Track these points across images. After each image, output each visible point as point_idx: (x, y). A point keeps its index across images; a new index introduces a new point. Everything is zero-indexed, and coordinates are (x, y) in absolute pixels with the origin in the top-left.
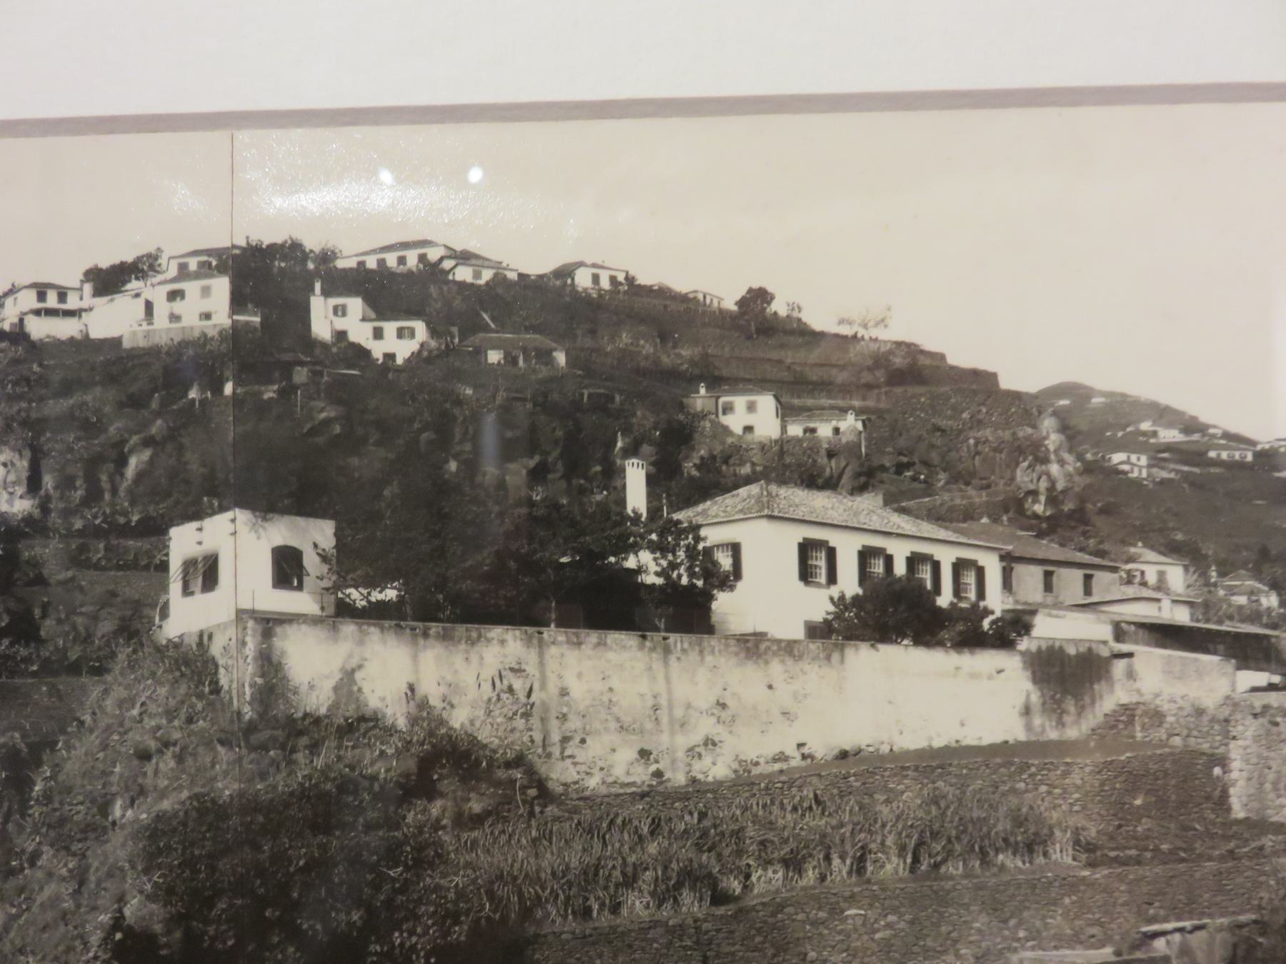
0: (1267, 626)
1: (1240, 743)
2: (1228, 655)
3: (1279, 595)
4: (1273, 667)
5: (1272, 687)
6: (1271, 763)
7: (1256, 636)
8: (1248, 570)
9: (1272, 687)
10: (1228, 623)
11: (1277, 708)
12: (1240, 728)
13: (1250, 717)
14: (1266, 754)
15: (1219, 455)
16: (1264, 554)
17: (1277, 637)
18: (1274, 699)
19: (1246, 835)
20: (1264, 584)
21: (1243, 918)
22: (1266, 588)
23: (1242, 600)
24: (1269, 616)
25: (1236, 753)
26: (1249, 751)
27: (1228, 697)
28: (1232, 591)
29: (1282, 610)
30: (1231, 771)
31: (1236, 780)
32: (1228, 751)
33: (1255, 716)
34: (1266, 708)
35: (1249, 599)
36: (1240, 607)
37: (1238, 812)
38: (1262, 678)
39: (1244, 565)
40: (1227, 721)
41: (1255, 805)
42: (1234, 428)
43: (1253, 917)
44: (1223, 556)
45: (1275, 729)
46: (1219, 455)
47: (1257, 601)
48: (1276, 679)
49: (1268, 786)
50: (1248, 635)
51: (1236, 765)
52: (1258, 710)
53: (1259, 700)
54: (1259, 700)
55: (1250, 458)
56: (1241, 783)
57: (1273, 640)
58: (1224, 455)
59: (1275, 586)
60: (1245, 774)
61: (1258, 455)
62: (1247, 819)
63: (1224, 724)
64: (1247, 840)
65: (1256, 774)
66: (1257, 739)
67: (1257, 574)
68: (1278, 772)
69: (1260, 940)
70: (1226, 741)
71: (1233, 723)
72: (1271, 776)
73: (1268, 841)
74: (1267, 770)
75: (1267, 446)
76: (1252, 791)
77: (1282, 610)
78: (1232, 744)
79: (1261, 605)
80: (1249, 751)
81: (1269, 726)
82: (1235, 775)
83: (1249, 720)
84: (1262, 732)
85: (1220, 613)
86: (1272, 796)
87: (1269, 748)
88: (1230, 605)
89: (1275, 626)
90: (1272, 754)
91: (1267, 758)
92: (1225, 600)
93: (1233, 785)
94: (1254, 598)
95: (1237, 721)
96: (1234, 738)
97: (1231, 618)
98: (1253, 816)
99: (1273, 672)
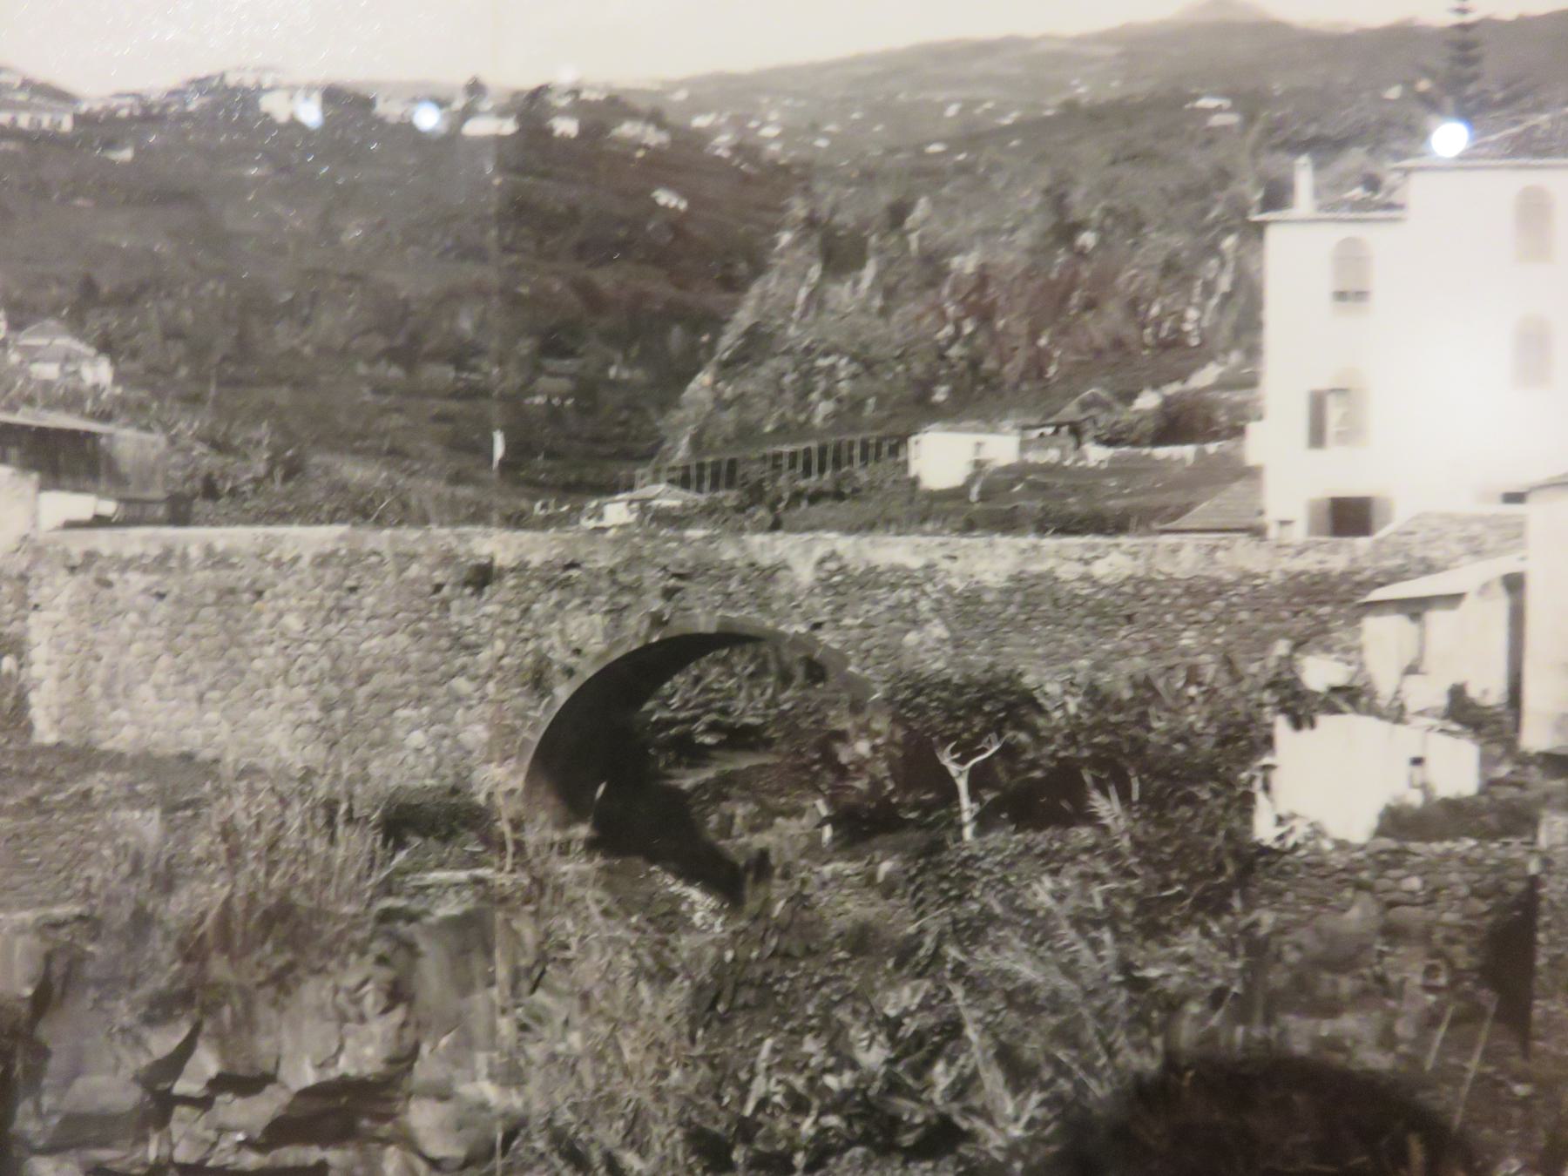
0: (93, 416)
1: (47, 615)
2: (27, 465)
3: (114, 362)
4: (103, 486)
5: (99, 521)
6: (100, 650)
7: (74, 435)
8: (61, 319)
9: (99, 521)
10: (24, 409)
11: (110, 557)
12: (46, 591)
13: (63, 573)
14: (90, 634)
15: (14, 120)
16: (89, 288)
17: (110, 436)
18: (103, 541)
19: (61, 772)
20: (90, 344)
21: (60, 911)
22: (91, 351)
23: (48, 371)
24: (97, 398)
25: (39, 631)
26: (61, 629)
27: (25, 538)
28: (31, 354)
29: (119, 390)
30: (31, 664)
31: (41, 681)
32: (27, 630)
33: (72, 569)
34: (90, 557)
35: (62, 368)
36: (47, 385)
37: (45, 732)
38: (83, 505)
39: (54, 310)
40: (23, 578)
41: (73, 721)
42: (44, 73)
43: (77, 910)
44: (17, 294)
45: (105, 594)
46: (14, 120)
47: (76, 373)
48: (108, 507)
49: (95, 690)
50: (60, 433)
51: (39, 653)
52: (77, 560)
53: (78, 543)
54: (78, 543)
55: (67, 124)
56: (49, 684)
57: (103, 441)
58: (24, 121)
59: (106, 346)
60: (55, 670)
61: (81, 120)
62: (59, 745)
63: (19, 584)
64: (61, 781)
65: (75, 668)
66: (74, 609)
67: (76, 324)
68: (114, 666)
69: (90, 948)
70: (22, 612)
71: (33, 582)
72: (100, 673)
73: (99, 782)
74: (91, 664)
75: (97, 107)
76: (68, 698)
77: (119, 390)
78: (33, 619)
79: (81, 380)
80: (61, 629)
81: (96, 588)
82: (37, 670)
83: (62, 577)
84: (84, 596)
85: (13, 393)
86: (102, 706)
87: (95, 625)
88: (28, 380)
89: (106, 417)
90: (101, 636)
91: (93, 643)
92: (20, 369)
93: (36, 687)
94: (70, 368)
95: (41, 579)
96: (36, 607)
97: (30, 401)
98: (71, 740)
99: (103, 495)
